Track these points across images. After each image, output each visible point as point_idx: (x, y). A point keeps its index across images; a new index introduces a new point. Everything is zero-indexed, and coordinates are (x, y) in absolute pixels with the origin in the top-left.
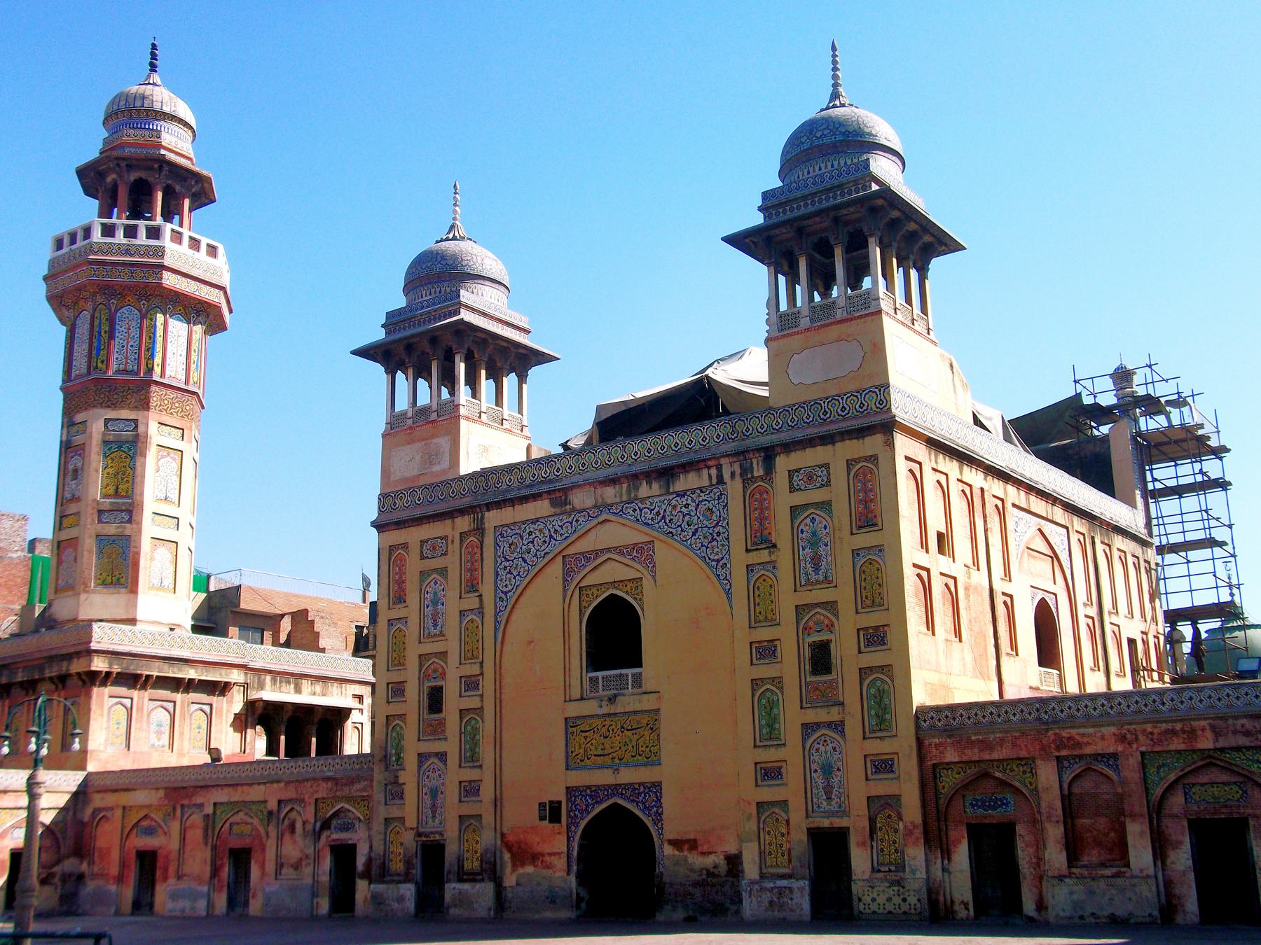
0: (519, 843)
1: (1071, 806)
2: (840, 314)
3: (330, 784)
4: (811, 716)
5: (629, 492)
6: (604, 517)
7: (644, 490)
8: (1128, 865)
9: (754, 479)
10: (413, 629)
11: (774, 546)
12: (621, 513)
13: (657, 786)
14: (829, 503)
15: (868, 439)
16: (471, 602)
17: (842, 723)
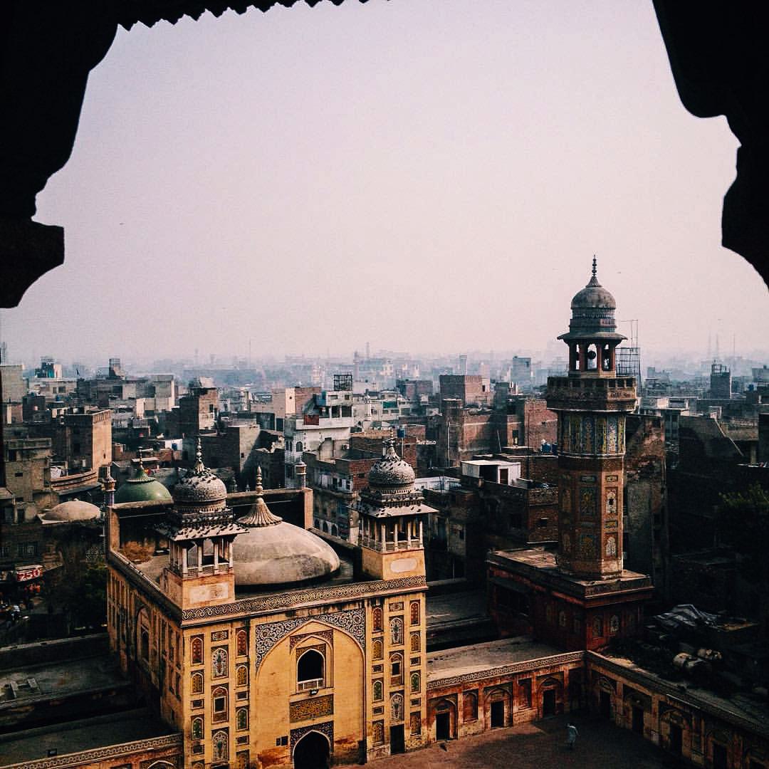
0: (266, 757)
1: (465, 703)
2: (409, 548)
3: (150, 754)
4: (393, 689)
5: (324, 610)
6: (312, 620)
7: (331, 610)
8: (477, 719)
9: (377, 606)
10: (208, 674)
11: (383, 631)
12: (319, 619)
13: (332, 722)
14: (403, 616)
15: (418, 595)
16: (243, 659)
17: (403, 691)
